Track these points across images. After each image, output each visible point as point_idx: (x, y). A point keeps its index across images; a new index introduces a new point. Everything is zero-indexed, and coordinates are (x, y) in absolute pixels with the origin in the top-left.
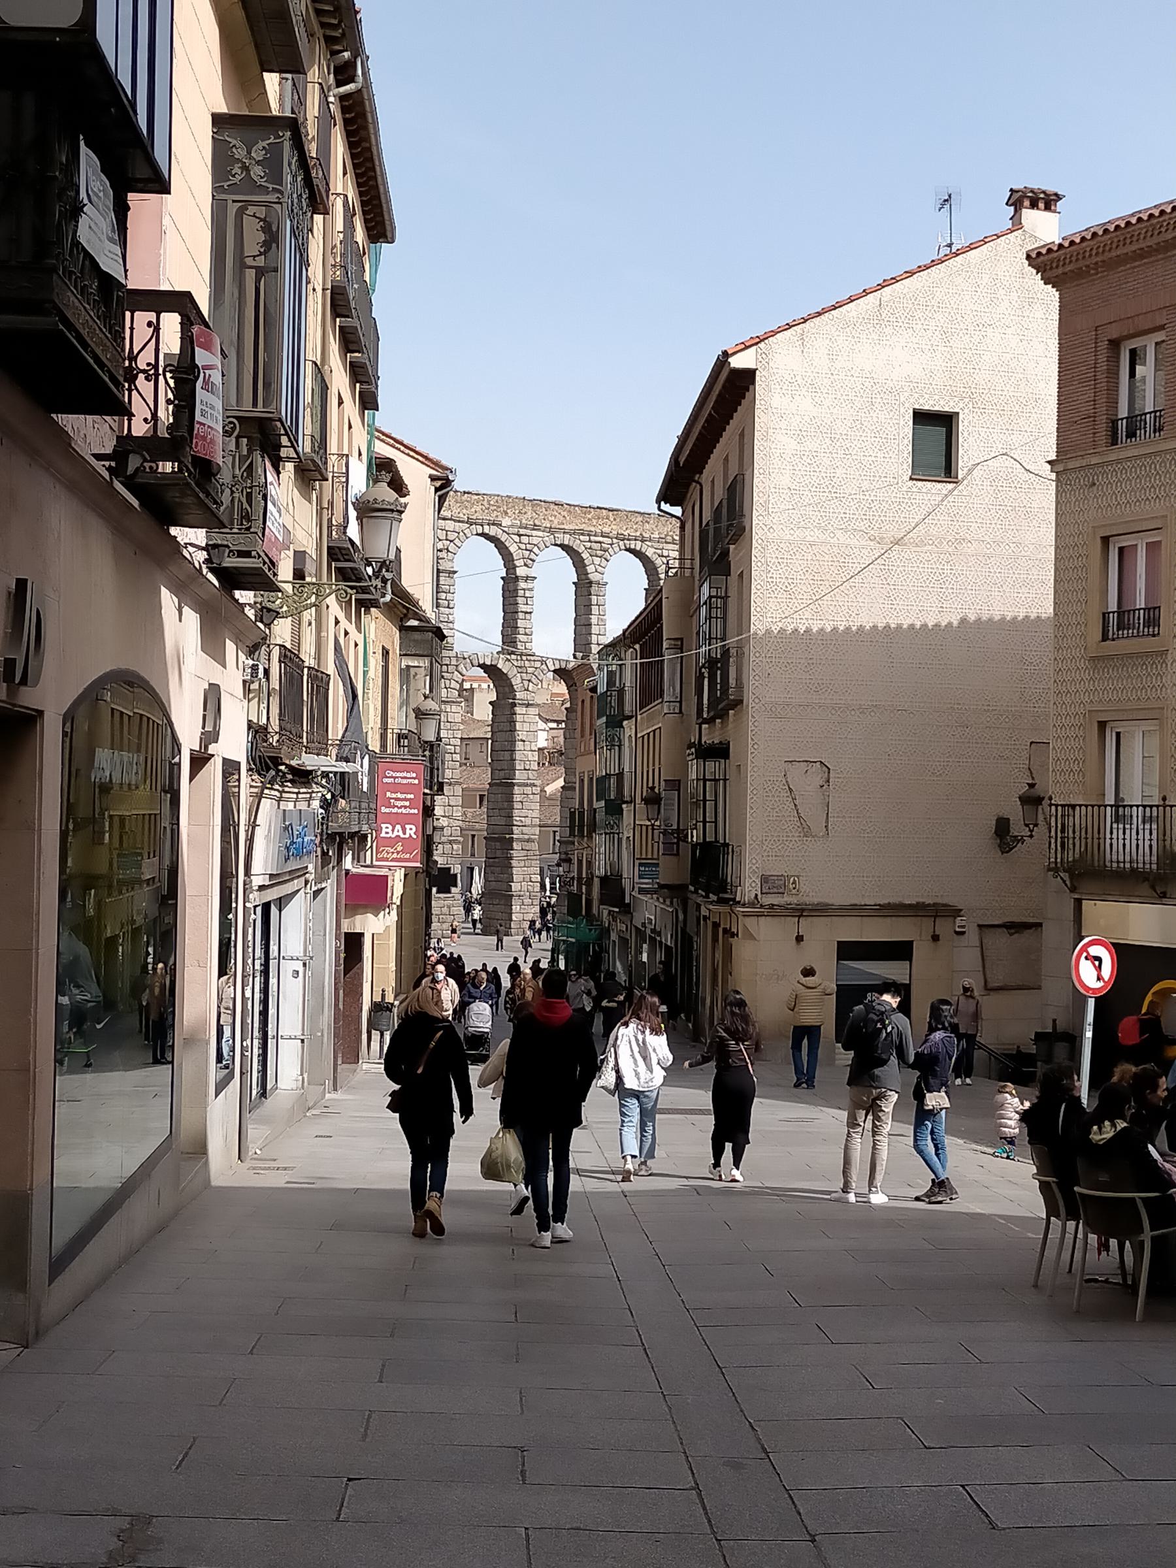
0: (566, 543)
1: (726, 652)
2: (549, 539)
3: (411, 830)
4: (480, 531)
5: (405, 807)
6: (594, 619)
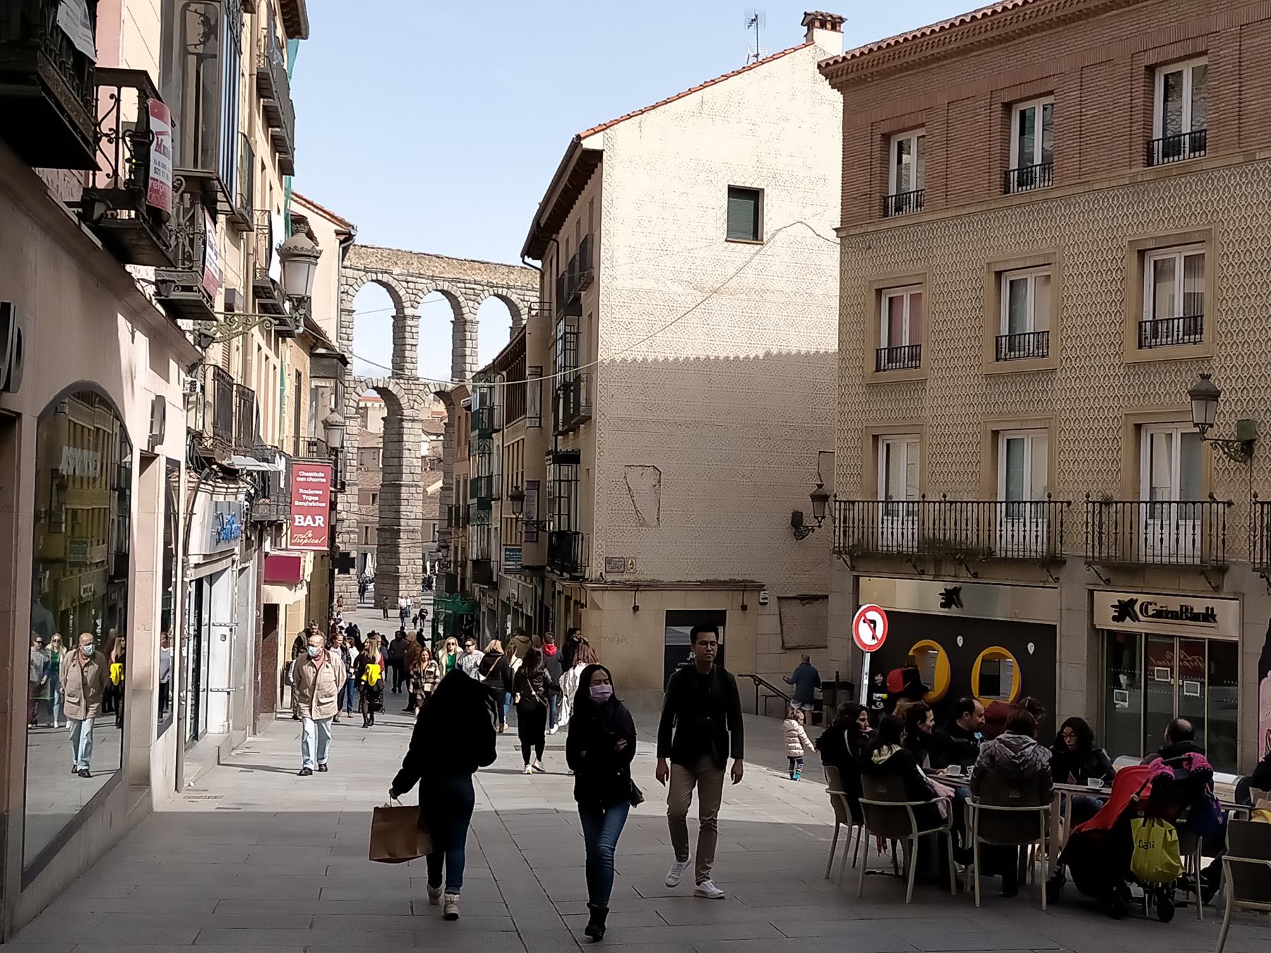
1: (578, 378)
2: (432, 286)
3: (320, 521)
6: (468, 352)
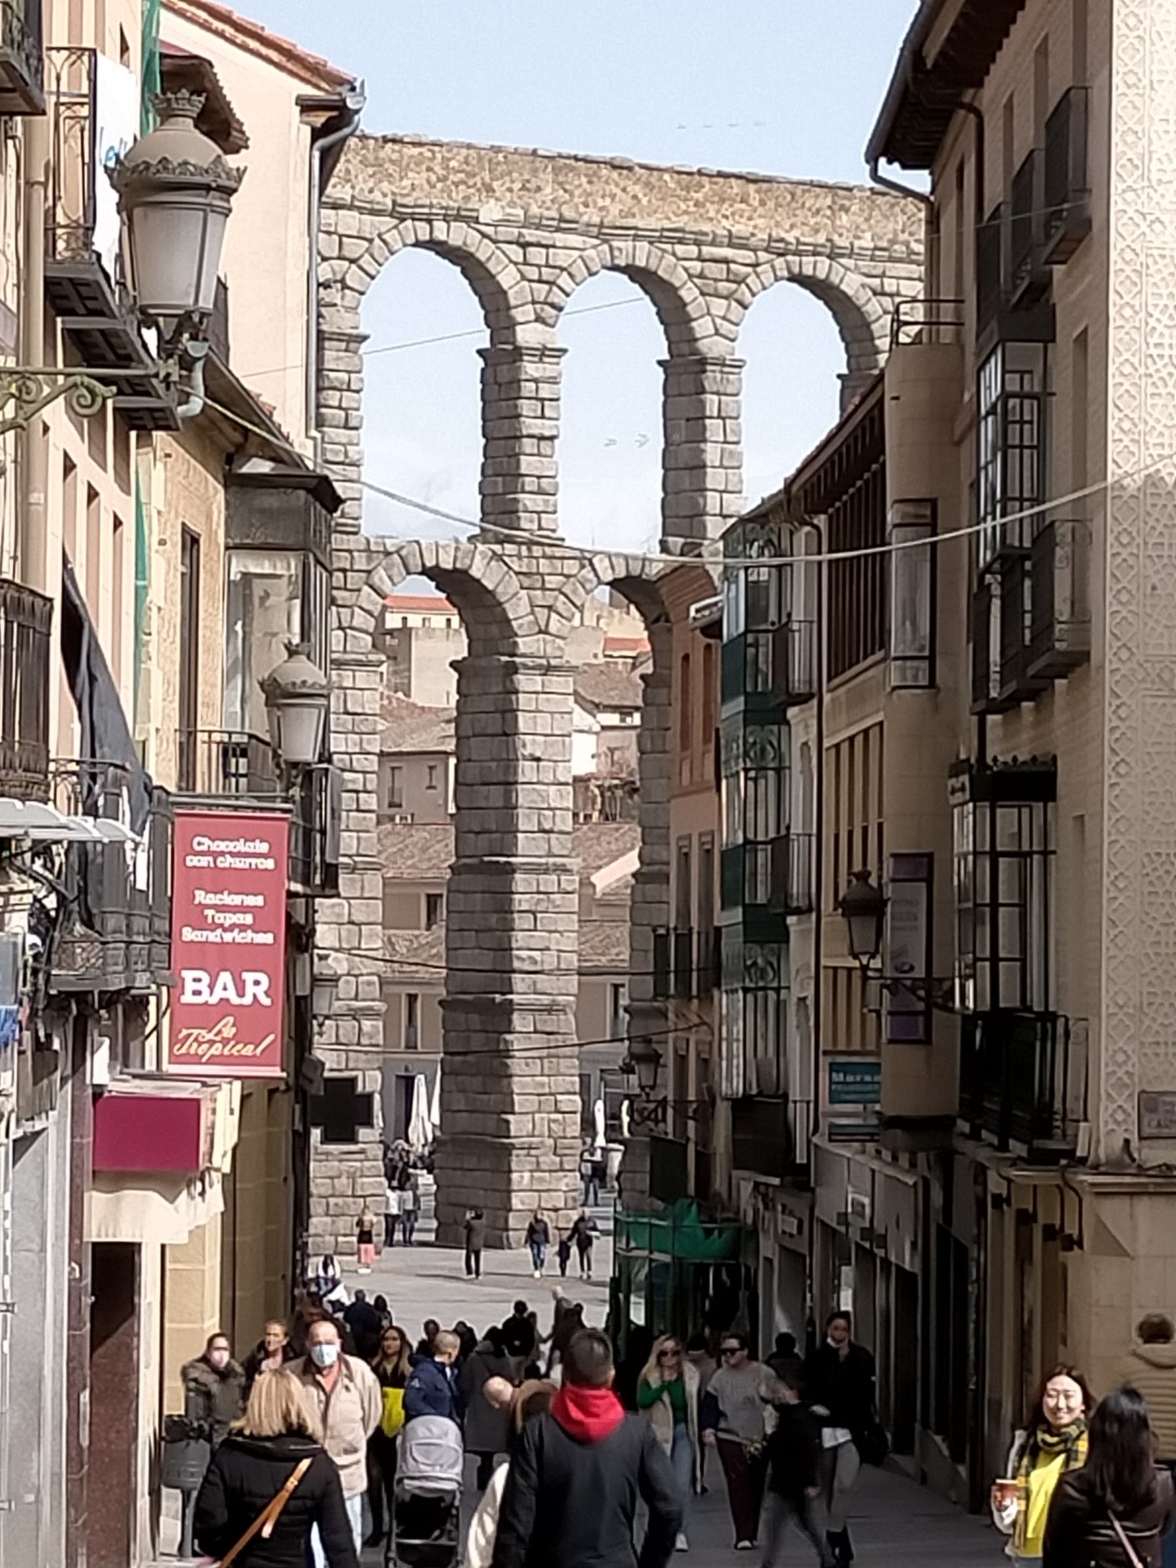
0: (641, 262)
1: (1045, 533)
2: (597, 253)
3: (259, 987)
4: (424, 236)
5: (243, 928)
6: (712, 454)
